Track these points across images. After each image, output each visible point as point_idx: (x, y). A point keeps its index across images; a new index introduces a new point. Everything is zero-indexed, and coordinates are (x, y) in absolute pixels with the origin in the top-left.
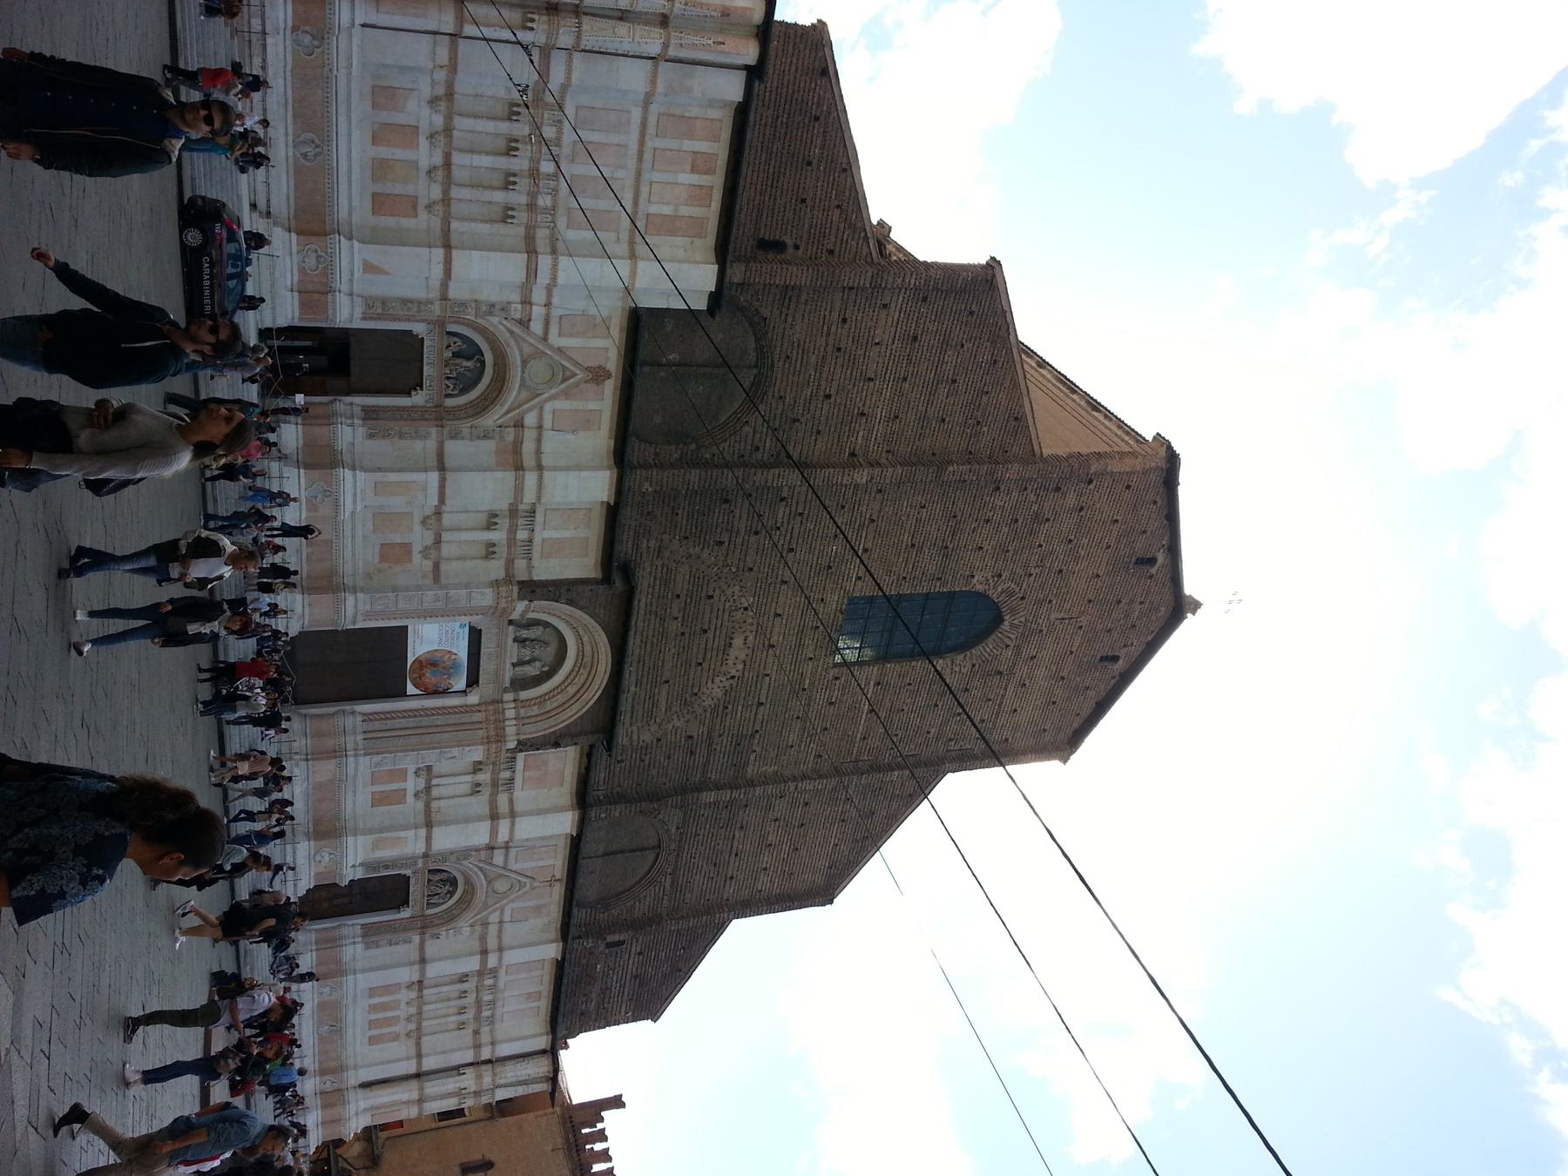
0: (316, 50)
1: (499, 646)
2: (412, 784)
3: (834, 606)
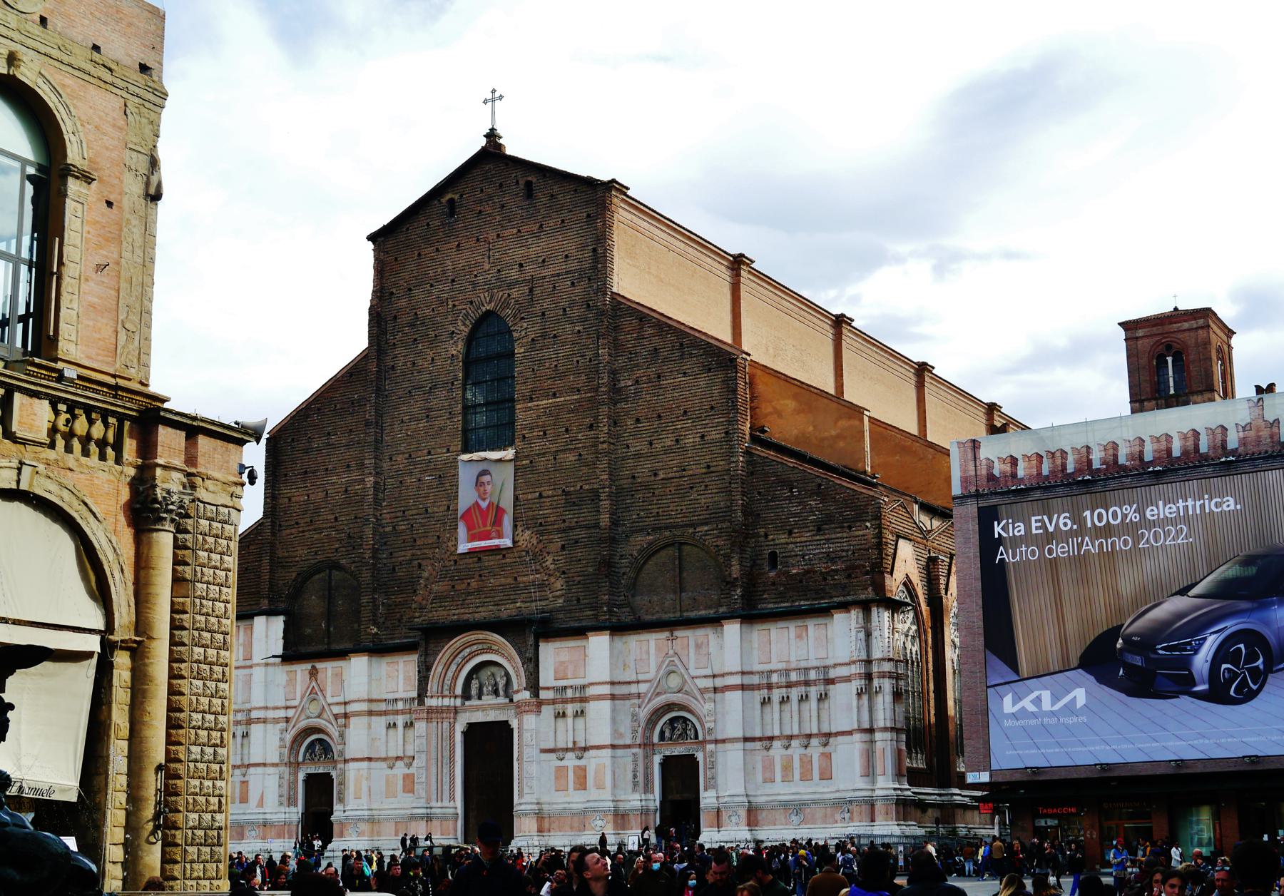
2: (570, 761)
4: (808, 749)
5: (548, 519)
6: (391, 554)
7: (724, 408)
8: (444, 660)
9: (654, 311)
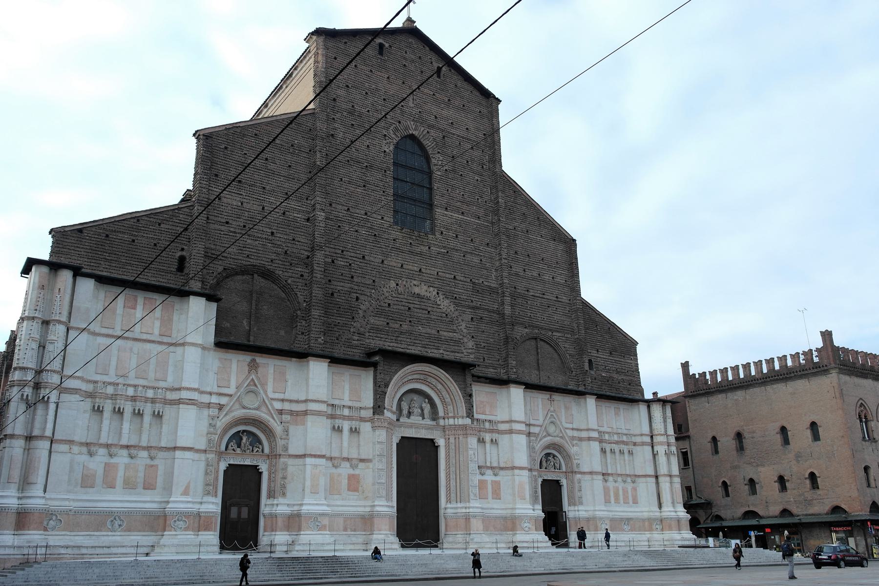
0: (58, 518)
1: (411, 427)
2: (489, 477)
3: (398, 233)
4: (626, 484)
5: (461, 296)
6: (330, 281)
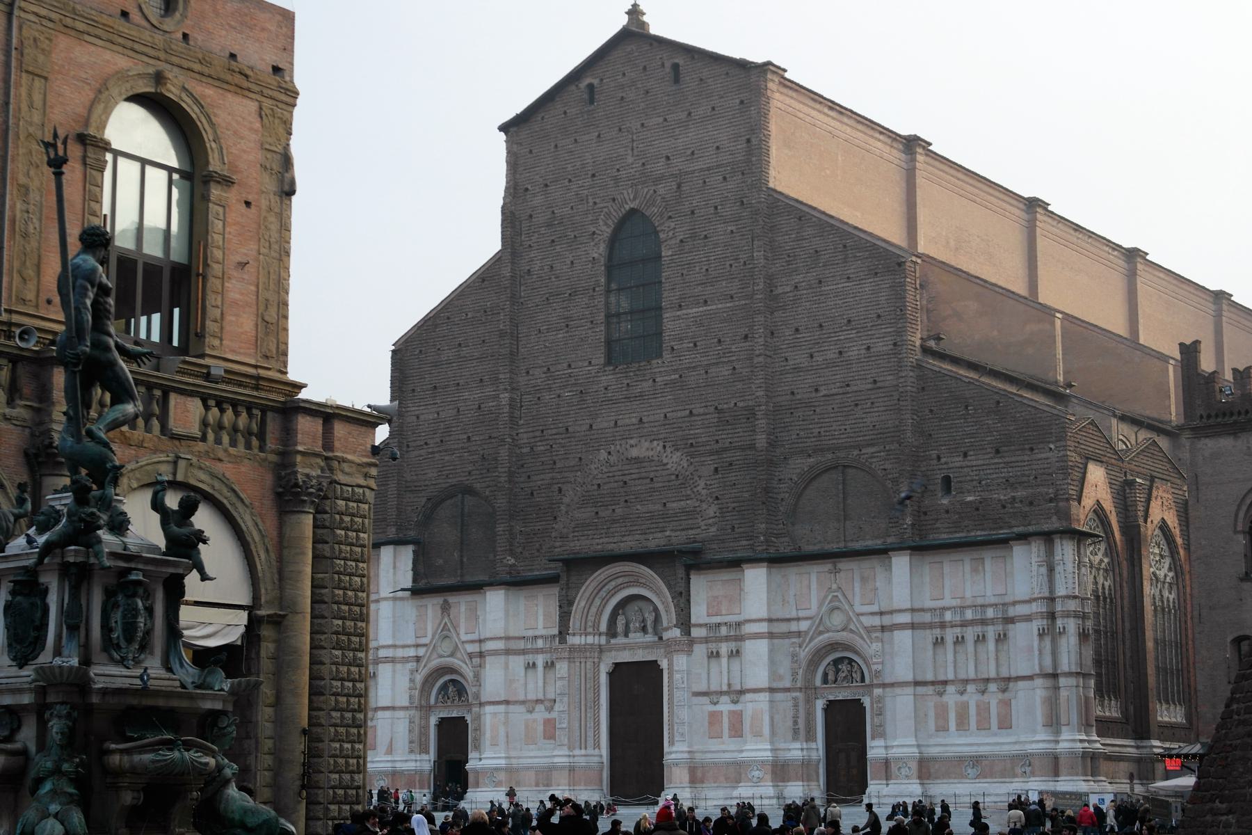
2: (725, 706)
3: (610, 377)
4: (986, 695)
5: (700, 440)
6: (529, 477)
7: (891, 317)
8: (587, 594)
9: (815, 209)
